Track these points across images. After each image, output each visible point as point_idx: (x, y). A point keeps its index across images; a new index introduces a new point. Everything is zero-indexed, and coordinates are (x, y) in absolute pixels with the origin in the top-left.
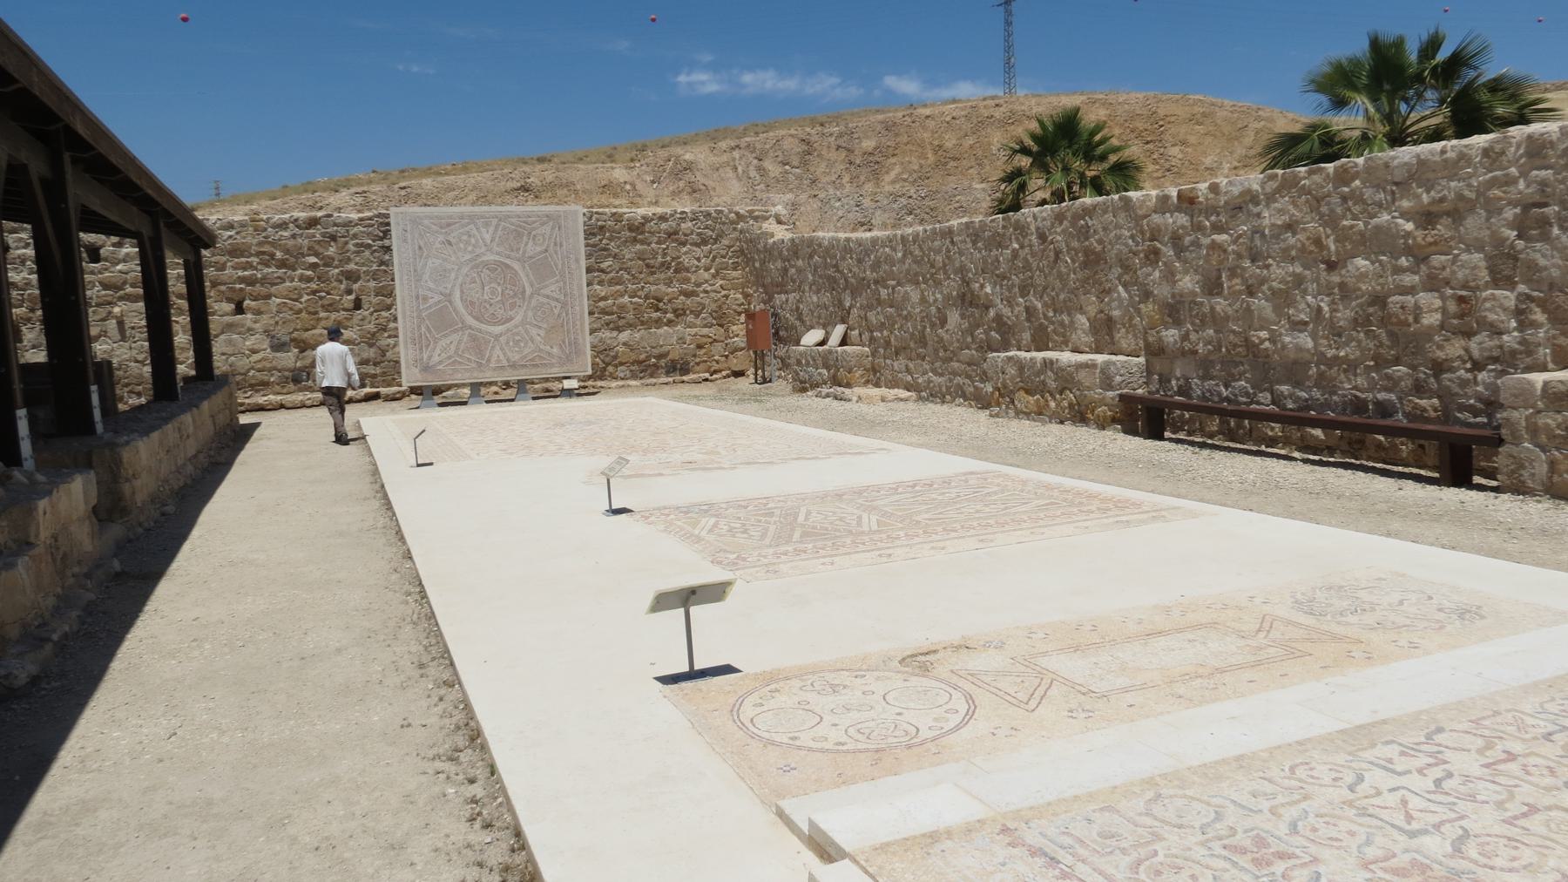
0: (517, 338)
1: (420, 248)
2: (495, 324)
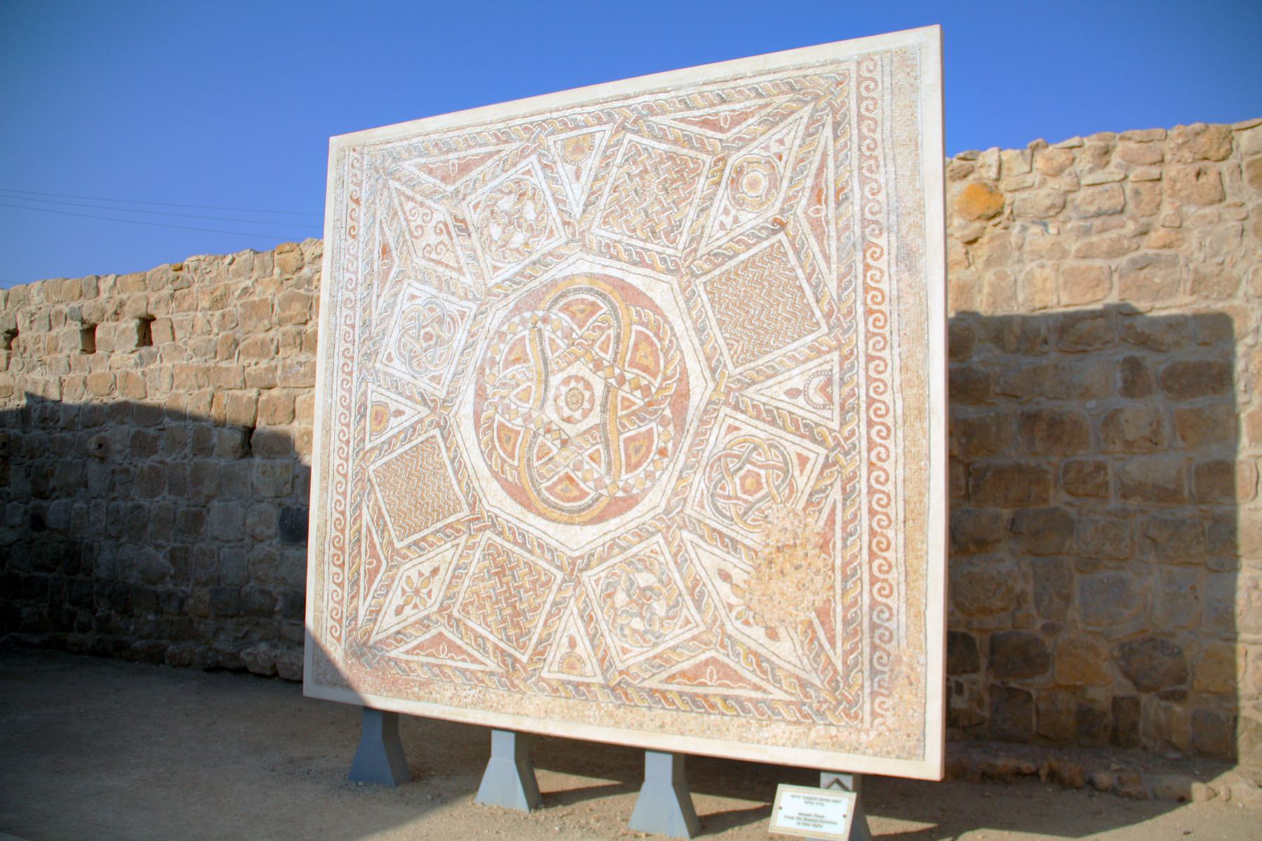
0: (644, 579)
1: (385, 251)
2: (572, 517)
